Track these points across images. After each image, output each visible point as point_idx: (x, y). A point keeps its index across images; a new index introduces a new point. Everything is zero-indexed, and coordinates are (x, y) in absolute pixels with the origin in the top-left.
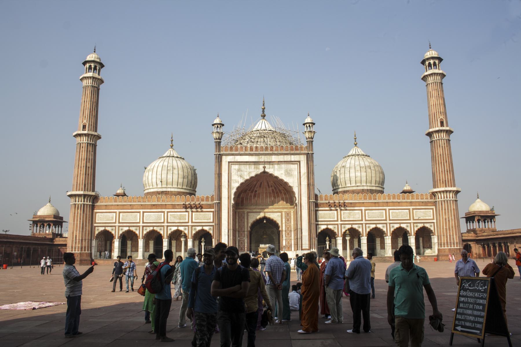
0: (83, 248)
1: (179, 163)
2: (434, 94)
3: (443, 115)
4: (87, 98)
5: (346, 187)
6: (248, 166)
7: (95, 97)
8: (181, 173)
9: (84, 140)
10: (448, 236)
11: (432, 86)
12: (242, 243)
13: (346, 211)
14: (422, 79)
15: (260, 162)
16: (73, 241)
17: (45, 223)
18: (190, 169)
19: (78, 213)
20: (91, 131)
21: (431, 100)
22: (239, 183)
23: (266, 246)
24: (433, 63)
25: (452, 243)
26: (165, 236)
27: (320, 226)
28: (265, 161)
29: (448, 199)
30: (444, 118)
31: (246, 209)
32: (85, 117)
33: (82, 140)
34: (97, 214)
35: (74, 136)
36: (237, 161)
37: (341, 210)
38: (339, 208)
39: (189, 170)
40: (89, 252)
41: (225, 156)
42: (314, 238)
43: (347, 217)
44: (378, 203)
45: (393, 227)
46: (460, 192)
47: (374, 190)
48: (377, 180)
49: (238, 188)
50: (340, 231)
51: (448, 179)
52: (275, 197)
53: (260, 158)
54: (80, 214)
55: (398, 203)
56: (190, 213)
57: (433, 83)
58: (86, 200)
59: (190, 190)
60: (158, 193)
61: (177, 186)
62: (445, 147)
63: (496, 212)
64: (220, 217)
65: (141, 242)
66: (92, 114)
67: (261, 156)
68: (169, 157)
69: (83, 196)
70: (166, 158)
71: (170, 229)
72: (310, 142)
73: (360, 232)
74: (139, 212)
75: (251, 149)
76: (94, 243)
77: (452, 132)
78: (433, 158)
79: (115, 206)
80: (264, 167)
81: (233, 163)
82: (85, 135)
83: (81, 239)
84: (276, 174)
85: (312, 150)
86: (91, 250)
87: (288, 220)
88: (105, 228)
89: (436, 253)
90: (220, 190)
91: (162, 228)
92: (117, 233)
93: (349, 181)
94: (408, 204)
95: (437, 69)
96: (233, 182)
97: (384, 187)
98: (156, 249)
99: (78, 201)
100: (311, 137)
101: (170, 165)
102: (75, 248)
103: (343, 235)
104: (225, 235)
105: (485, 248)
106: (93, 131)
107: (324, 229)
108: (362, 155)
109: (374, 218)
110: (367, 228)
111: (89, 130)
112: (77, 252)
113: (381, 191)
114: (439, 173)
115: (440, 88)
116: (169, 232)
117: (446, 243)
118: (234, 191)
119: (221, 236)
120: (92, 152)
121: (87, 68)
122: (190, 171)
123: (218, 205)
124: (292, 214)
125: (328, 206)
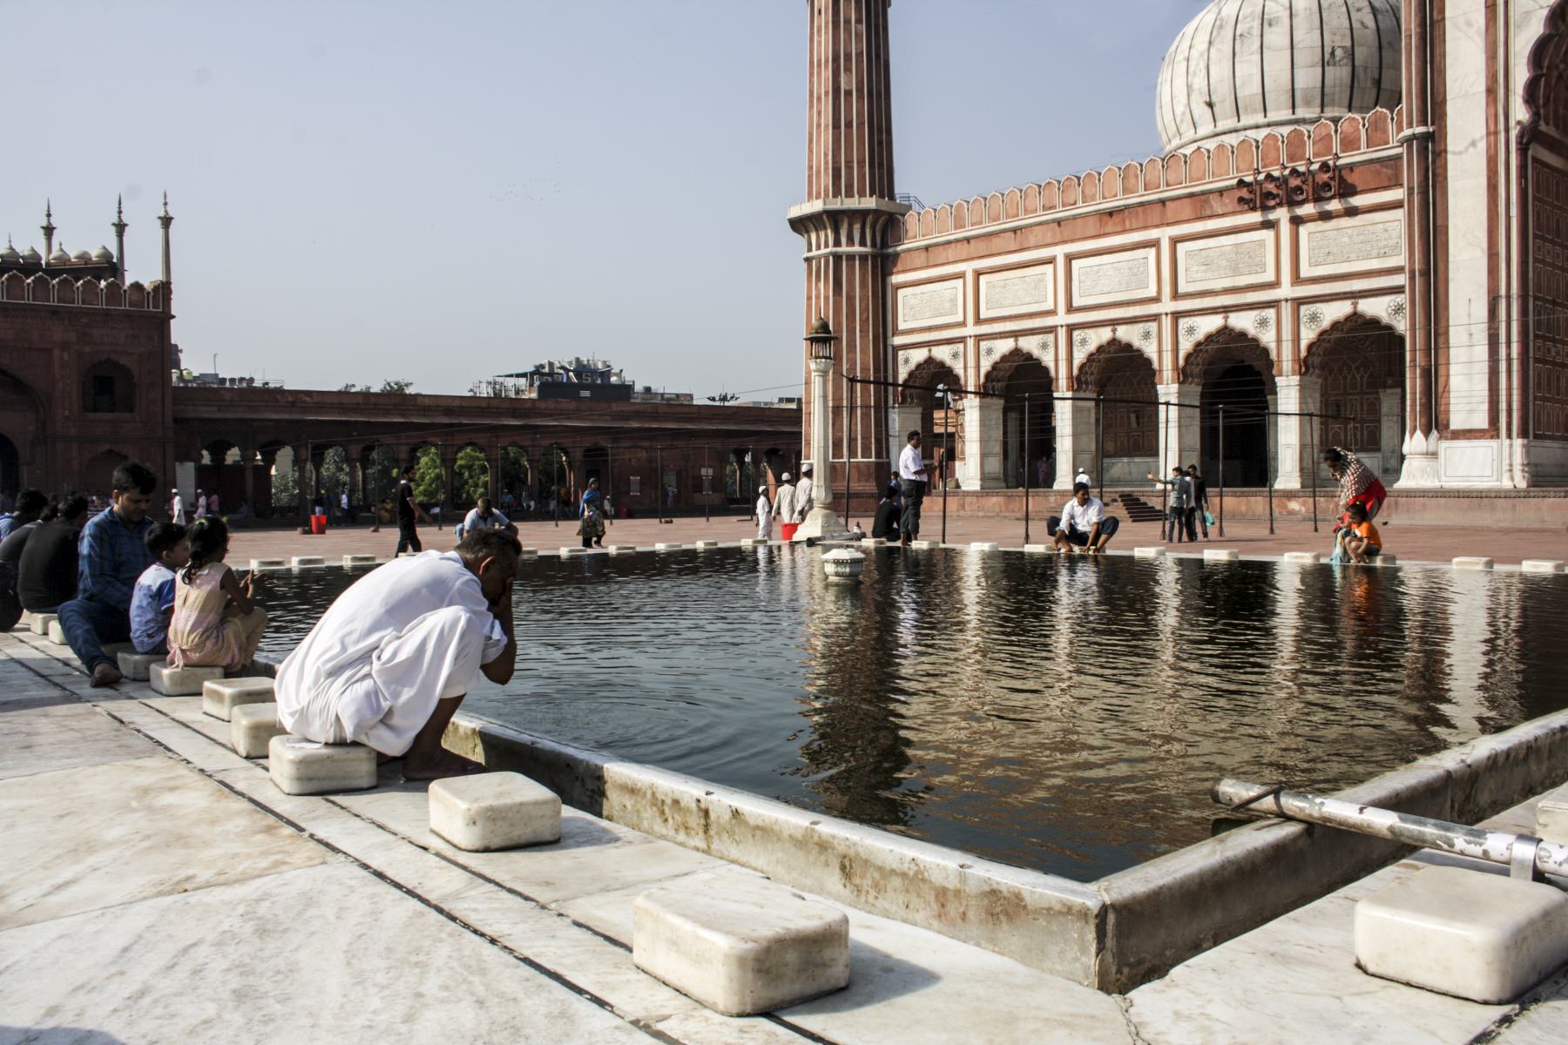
8: (1307, 38)
18: (1368, 10)
19: (818, 297)
34: (901, 293)
40: (873, 459)
56: (1285, 227)
61: (1294, 113)
71: (1191, 330)
74: (1051, 261)
79: (959, 245)
88: (930, 351)
90: (1437, 52)
91: (1153, 326)
99: (818, 248)
104: (1471, 335)
116: (1186, 345)
120: (859, 21)
123: (1423, 151)
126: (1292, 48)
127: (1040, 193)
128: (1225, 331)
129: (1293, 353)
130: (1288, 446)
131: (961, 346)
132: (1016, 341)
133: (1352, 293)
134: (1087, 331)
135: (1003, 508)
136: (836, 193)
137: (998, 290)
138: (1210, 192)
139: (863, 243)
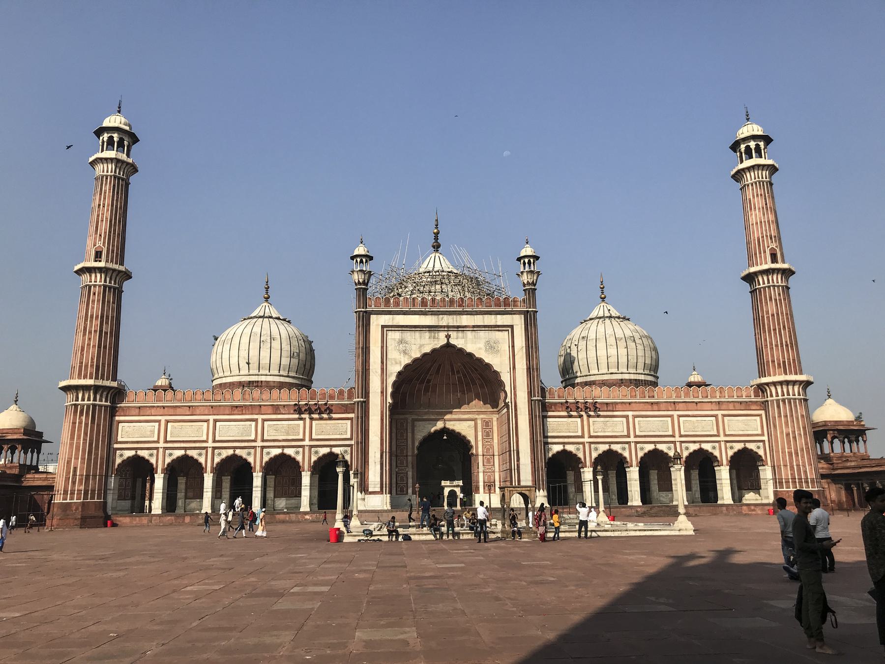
0: (90, 492)
1: (284, 330)
2: (759, 203)
3: (776, 242)
4: (105, 198)
5: (590, 375)
6: (417, 334)
7: (121, 198)
8: (286, 347)
9: (98, 279)
10: (795, 467)
11: (753, 189)
12: (402, 478)
13: (598, 419)
14: (733, 177)
15: (441, 327)
16: (67, 479)
17: (5, 444)
18: (302, 340)
19: (80, 423)
20: (113, 263)
21: (752, 215)
22: (401, 365)
23: (453, 483)
24: (754, 146)
25: (803, 480)
26: (258, 468)
27: (550, 446)
28: (449, 325)
29: (791, 396)
30: (776, 247)
31: (411, 413)
32: (100, 235)
33: (93, 280)
35: (76, 272)
36: (398, 324)
37: (589, 416)
38: (586, 413)
39: (302, 342)
40: (102, 500)
41: (375, 316)
42: (542, 469)
43: (600, 430)
44: (657, 403)
45: (687, 448)
46: (812, 383)
47: (642, 380)
48: (646, 362)
49: (400, 373)
50: (589, 454)
51: (789, 359)
52: (463, 392)
53: (440, 319)
54: (86, 425)
55: (695, 404)
56: (308, 421)
57: (756, 183)
58: (98, 397)
59: (302, 379)
60: (241, 384)
61: (279, 372)
62: (780, 300)
63: (866, 423)
64: (366, 428)
65: (208, 480)
66: (115, 230)
67: (441, 316)
68: (263, 317)
69: (93, 388)
70: (257, 319)
71: (268, 453)
72: (531, 291)
73: (625, 458)
74: (207, 421)
75: (424, 303)
76: (112, 482)
77: (793, 273)
78: (758, 321)
79: (158, 409)
80: (448, 337)
81: (390, 329)
82: (100, 270)
83: (85, 474)
84: (469, 349)
85: (535, 306)
86: (105, 498)
87: (488, 435)
88: (136, 452)
89: (771, 499)
91: (252, 451)
92: (160, 461)
93: (596, 364)
94: (714, 406)
95: (761, 157)
96: (390, 363)
97: (658, 375)
98: (234, 493)
99: (83, 400)
100: (533, 281)
101: (265, 333)
102: (72, 493)
103: (594, 463)
105: (852, 491)
106: (116, 263)
107: (558, 452)
108: (617, 317)
109: (650, 431)
110: (638, 449)
111: (107, 261)
112: (75, 501)
113: (654, 382)
114: (772, 349)
115: (768, 193)
116: (266, 459)
117: (790, 480)
118: (392, 379)
119: (368, 465)
120: (113, 303)
121: (103, 142)
122: (304, 345)
124: (495, 423)
125: (564, 408)
126: (281, 350)
127: (203, 394)
128: (283, 455)
129: (309, 464)
130: (305, 496)
131: (155, 451)
132: (186, 451)
133: (330, 445)
134: (221, 450)
135: (174, 521)
136: (97, 378)
137: (177, 430)
138: (280, 405)
139: (106, 401)
